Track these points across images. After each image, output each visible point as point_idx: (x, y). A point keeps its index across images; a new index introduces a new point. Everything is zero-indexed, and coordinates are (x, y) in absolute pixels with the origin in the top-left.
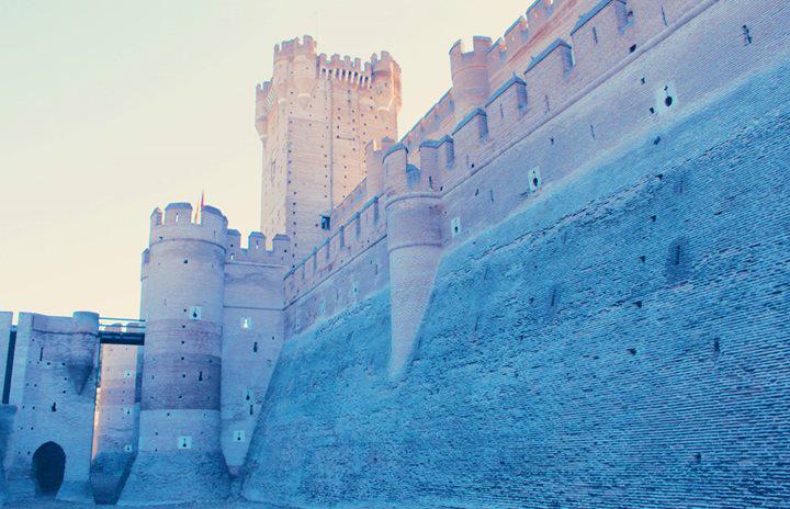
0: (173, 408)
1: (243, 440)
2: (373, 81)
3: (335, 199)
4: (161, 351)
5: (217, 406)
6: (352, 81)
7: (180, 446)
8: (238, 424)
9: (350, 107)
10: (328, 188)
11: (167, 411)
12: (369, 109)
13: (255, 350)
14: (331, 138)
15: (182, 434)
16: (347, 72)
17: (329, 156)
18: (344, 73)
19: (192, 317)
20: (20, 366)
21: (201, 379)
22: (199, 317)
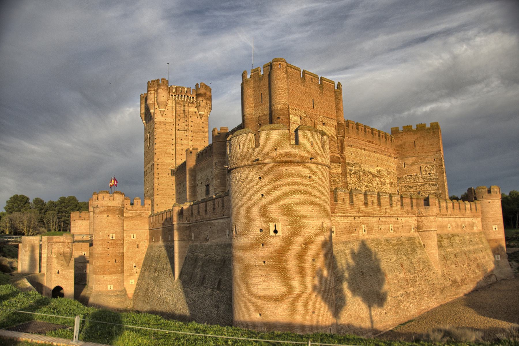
0: (106, 274)
1: (133, 283)
2: (197, 99)
3: (177, 161)
4: (100, 252)
5: (122, 272)
6: (186, 100)
7: (109, 289)
8: (132, 277)
9: (184, 114)
10: (174, 156)
11: (103, 276)
12: (194, 113)
13: (138, 247)
14: (175, 131)
15: (109, 284)
16: (183, 96)
17: (174, 140)
18: (182, 96)
19: (111, 238)
20: (45, 257)
21: (116, 262)
22: (114, 238)
